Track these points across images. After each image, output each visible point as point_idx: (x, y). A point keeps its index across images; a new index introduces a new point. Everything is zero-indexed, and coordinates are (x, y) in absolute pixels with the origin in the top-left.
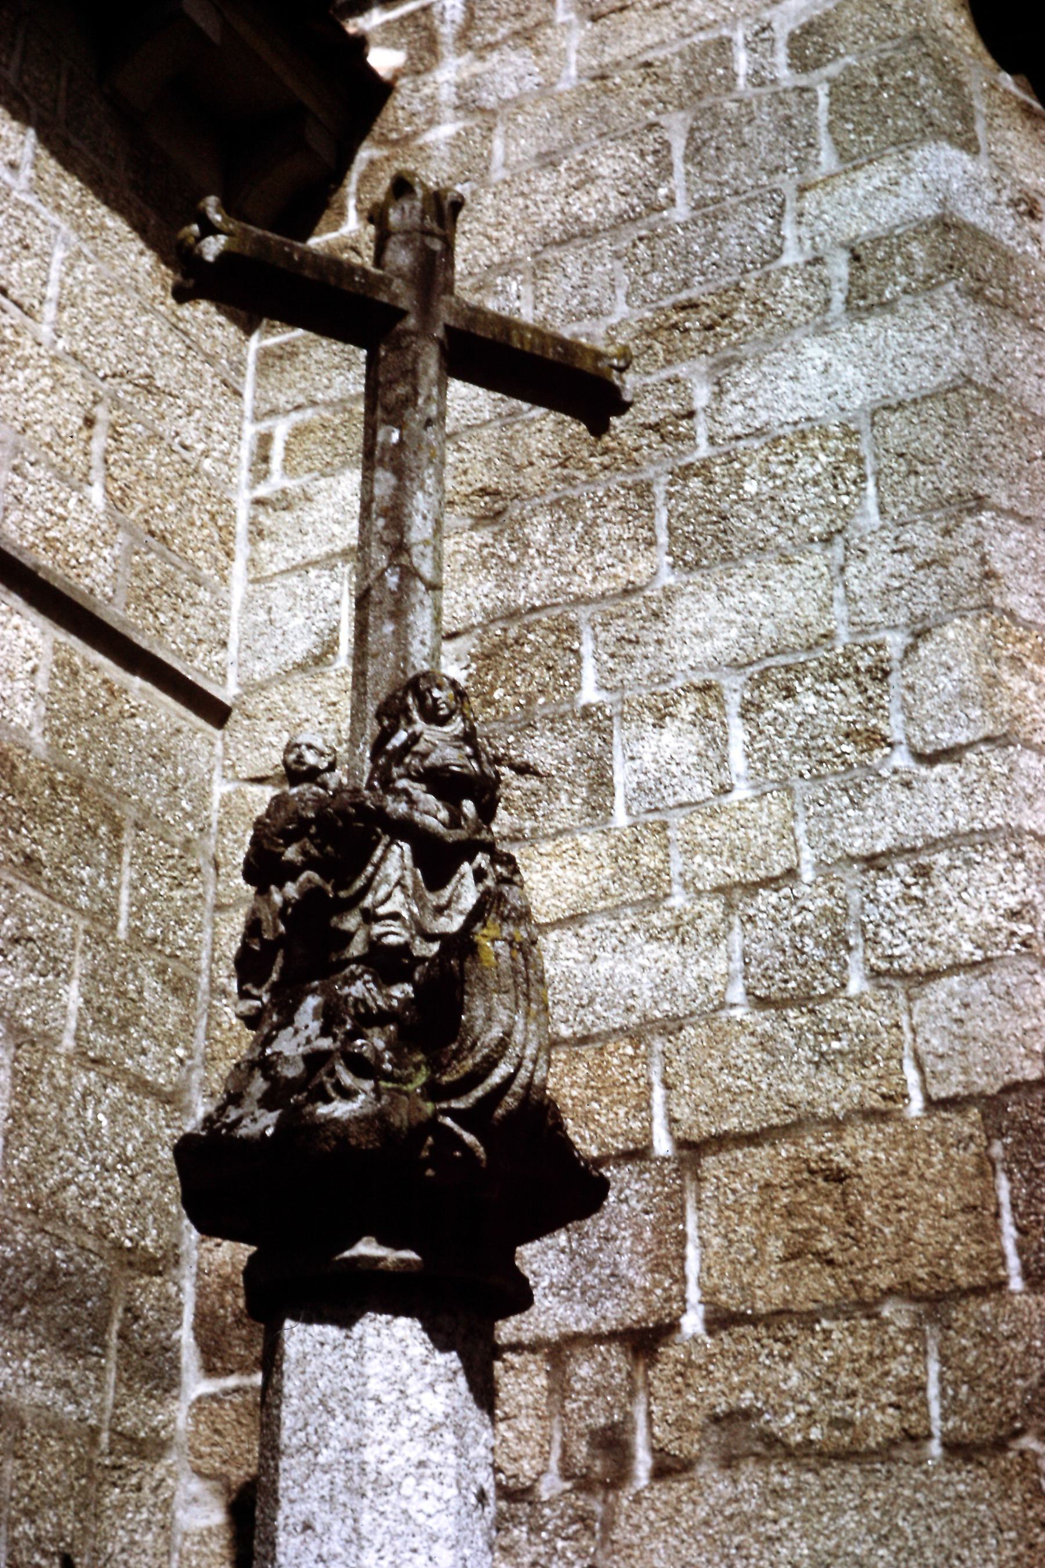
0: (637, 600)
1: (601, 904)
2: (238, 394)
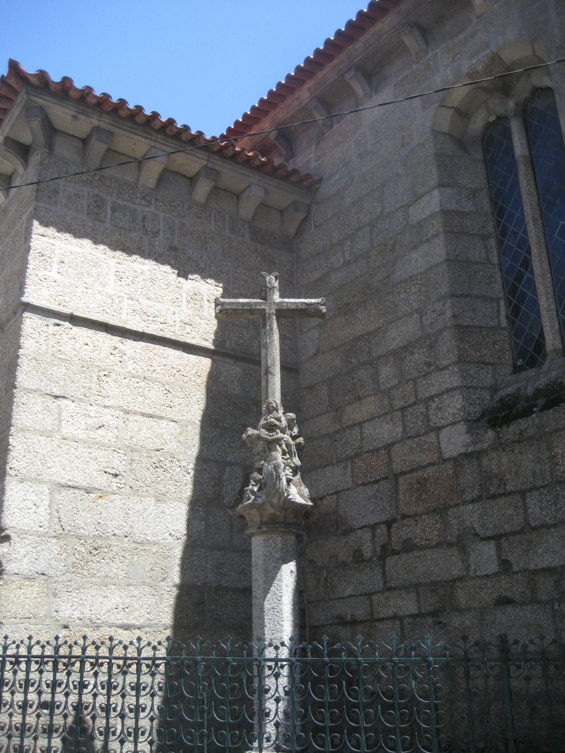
1: (376, 415)
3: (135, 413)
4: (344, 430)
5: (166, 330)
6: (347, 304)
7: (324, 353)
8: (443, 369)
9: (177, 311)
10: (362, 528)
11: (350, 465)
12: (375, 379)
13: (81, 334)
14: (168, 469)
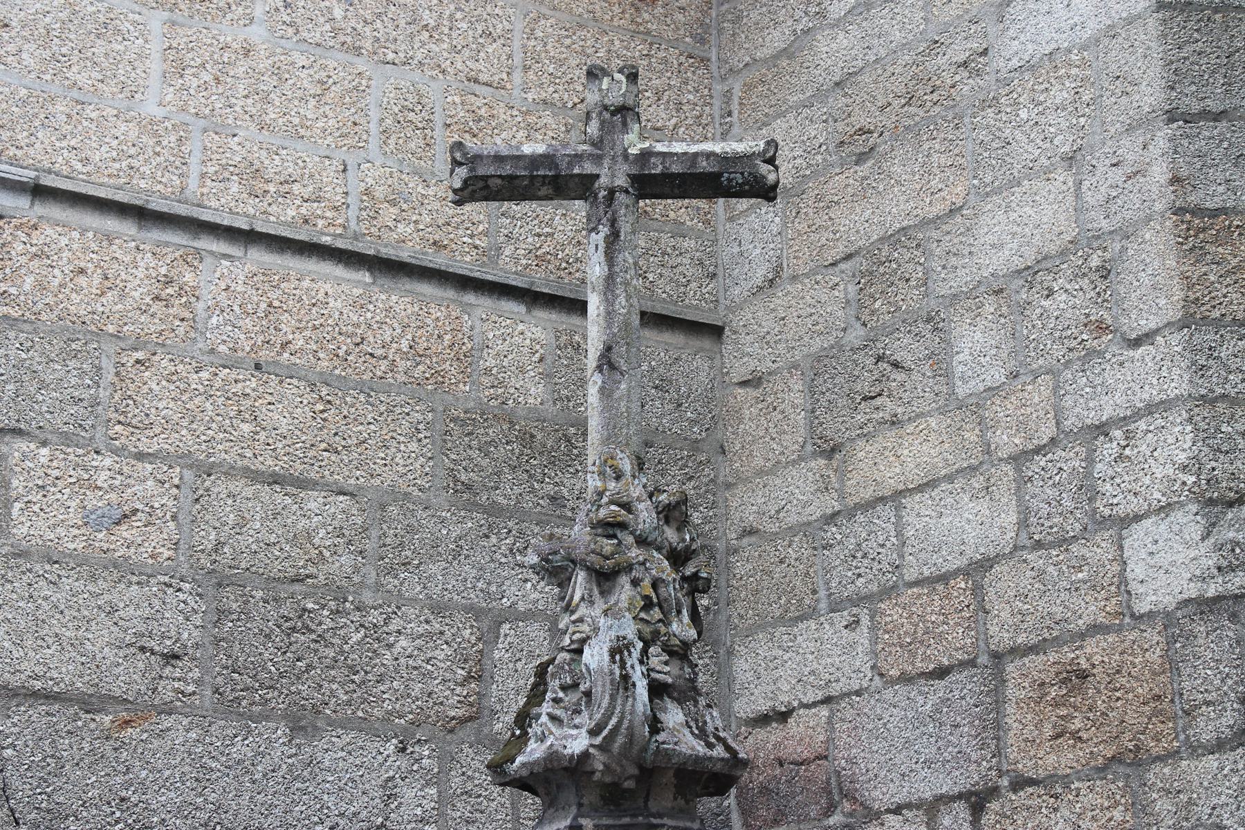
0: (959, 219)
2: (705, 60)
3: (230, 472)
4: (851, 513)
5: (320, 223)
6: (862, 131)
7: (794, 278)
8: (1136, 343)
9: (351, 163)
10: (897, 810)
11: (865, 621)
12: (940, 365)
13: (64, 241)
14: (327, 636)
